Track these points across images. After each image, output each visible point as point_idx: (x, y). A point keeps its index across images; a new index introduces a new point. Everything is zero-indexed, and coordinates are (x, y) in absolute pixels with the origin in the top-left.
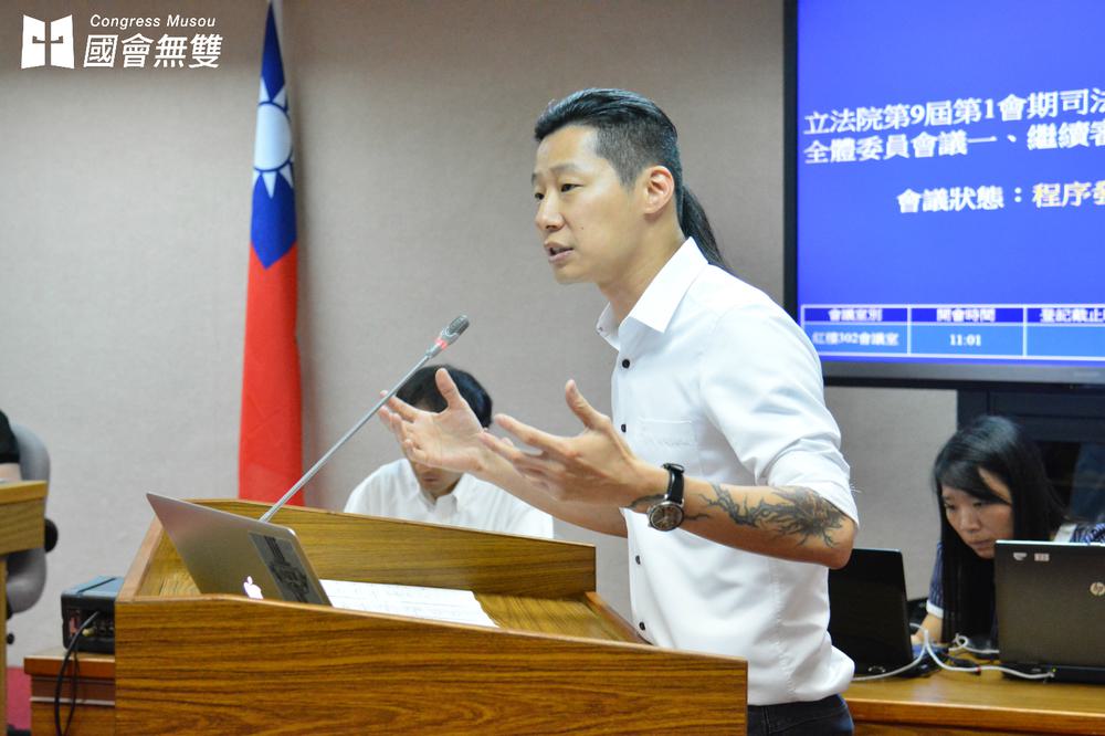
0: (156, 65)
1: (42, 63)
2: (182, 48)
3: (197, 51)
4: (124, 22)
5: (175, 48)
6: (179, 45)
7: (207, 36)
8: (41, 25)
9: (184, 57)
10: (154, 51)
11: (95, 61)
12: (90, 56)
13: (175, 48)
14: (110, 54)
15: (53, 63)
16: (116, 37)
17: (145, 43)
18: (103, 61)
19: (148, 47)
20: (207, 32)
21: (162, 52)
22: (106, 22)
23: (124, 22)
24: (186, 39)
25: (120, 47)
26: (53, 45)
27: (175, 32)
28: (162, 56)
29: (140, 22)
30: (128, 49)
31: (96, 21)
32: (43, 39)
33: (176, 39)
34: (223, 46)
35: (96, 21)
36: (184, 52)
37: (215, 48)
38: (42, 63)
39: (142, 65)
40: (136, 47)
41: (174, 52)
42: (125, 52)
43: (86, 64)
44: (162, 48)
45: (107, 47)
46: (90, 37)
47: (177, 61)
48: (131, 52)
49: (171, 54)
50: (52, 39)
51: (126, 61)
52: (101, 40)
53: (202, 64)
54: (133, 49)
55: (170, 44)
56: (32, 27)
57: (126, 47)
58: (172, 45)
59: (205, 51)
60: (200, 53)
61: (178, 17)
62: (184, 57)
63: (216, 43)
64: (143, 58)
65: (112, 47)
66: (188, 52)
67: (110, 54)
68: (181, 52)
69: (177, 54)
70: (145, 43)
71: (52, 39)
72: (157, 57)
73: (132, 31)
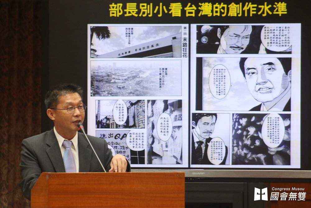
0: (289, 200)
1: (259, 199)
2: (296, 195)
3: (300, 197)
4: (281, 189)
5: (294, 196)
7: (302, 193)
8: (260, 190)
9: (296, 198)
10: (288, 196)
11: (273, 199)
12: (272, 197)
13: (294, 196)
14: (277, 197)
15: (262, 199)
16: (279, 193)
17: (286, 194)
18: (275, 199)
19: (287, 195)
20: (302, 191)
22: (276, 189)
25: (280, 195)
26: (262, 195)
27: (294, 192)
29: (285, 189)
32: (260, 193)
33: (294, 193)
36: (296, 197)
38: (259, 199)
39: (285, 200)
40: (284, 195)
41: (294, 197)
42: (281, 197)
43: (271, 200)
44: (291, 196)
45: (276, 195)
46: (272, 193)
47: (294, 199)
48: (282, 196)
49: (293, 197)
51: (281, 199)
52: (275, 194)
53: (301, 200)
55: (293, 194)
56: (257, 190)
57: (281, 195)
59: (302, 196)
61: (295, 188)
62: (296, 198)
63: (304, 194)
67: (277, 197)
68: (295, 197)
69: (294, 197)
70: (286, 194)
73: (283, 191)
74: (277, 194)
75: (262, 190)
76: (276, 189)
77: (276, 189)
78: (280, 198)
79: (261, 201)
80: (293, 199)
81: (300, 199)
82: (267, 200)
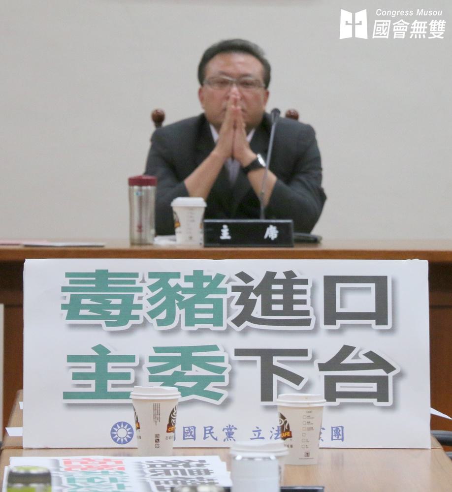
0: (411, 37)
1: (350, 36)
2: (425, 27)
3: (433, 30)
4: (394, 13)
5: (421, 27)
6: (423, 26)
8: (351, 14)
9: (426, 32)
10: (410, 30)
11: (379, 35)
12: (376, 32)
13: (421, 27)
14: (387, 31)
15: (357, 36)
16: (390, 21)
17: (405, 25)
18: (383, 35)
19: (406, 27)
20: (437, 18)
21: (414, 30)
22: (385, 13)
23: (394, 13)
24: (426, 22)
25: (392, 27)
26: (356, 26)
27: (421, 18)
29: (402, 13)
30: (396, 28)
31: (379, 12)
32: (351, 23)
33: (421, 23)
35: (379, 12)
37: (442, 28)
38: (350, 36)
39: (403, 37)
40: (400, 27)
41: (420, 30)
42: (394, 30)
43: (374, 37)
44: (414, 28)
45: (385, 27)
46: (376, 21)
47: (422, 35)
48: (397, 30)
49: (419, 31)
50: (356, 23)
51: (395, 34)
52: (382, 23)
53: (435, 36)
55: (418, 25)
56: (346, 16)
57: (395, 27)
58: (419, 26)
59: (437, 29)
60: (434, 30)
61: (422, 10)
62: (426, 32)
63: (442, 25)
64: (404, 33)
65: (387, 26)
66: (428, 30)
67: (387, 31)
68: (424, 30)
69: (422, 31)
70: (405, 25)
71: (356, 23)
72: (411, 32)
73: (398, 18)
74: (387, 25)
79: (354, 39)
80: (420, 36)
81: (433, 36)
82: (366, 37)
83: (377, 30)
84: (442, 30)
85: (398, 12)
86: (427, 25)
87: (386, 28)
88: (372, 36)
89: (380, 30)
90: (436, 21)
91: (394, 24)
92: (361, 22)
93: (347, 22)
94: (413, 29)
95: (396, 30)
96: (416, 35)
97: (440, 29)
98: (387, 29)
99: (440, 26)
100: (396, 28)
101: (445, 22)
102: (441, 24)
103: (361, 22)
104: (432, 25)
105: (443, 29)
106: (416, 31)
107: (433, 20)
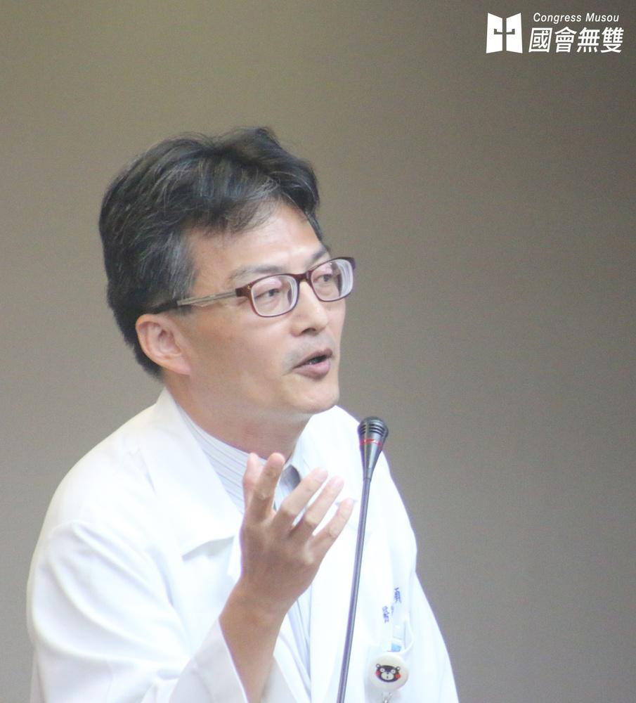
0: (578, 51)
1: (501, 49)
2: (596, 37)
4: (556, 19)
5: (591, 38)
6: (594, 35)
7: (614, 29)
8: (501, 19)
9: (597, 44)
10: (577, 41)
11: (537, 48)
12: (533, 43)
13: (591, 38)
14: (547, 42)
16: (551, 29)
17: (571, 34)
18: (542, 48)
19: (573, 37)
20: (613, 25)
21: (583, 41)
23: (556, 19)
24: (599, 31)
25: (554, 37)
26: (508, 36)
27: (591, 26)
28: (582, 44)
29: (567, 18)
30: (559, 39)
33: (592, 31)
34: (625, 37)
35: (537, 19)
36: (598, 41)
37: (619, 38)
38: (501, 49)
39: (569, 51)
40: (565, 37)
43: (530, 50)
44: (582, 38)
45: (545, 37)
46: (533, 29)
47: (593, 47)
48: (561, 41)
49: (589, 42)
51: (558, 47)
52: (540, 32)
53: (610, 50)
54: (563, 39)
55: (588, 34)
56: (494, 22)
57: (558, 37)
58: (590, 35)
59: (612, 40)
60: (608, 41)
61: (593, 14)
62: (597, 44)
63: (619, 34)
64: (570, 45)
65: (548, 36)
66: (600, 41)
67: (547, 42)
69: (593, 42)
70: (571, 34)
72: (579, 44)
75: (507, 19)
76: (544, 18)
77: (544, 18)
78: (554, 45)
79: (504, 54)
81: (606, 48)
82: (520, 51)
83: (535, 41)
84: (618, 41)
85: (562, 17)
86: (599, 34)
87: (546, 38)
88: (528, 50)
89: (539, 41)
90: (611, 28)
91: (556, 33)
92: (513, 30)
93: (495, 30)
94: (581, 40)
95: (559, 41)
96: (585, 48)
97: (616, 40)
98: (548, 39)
99: (617, 36)
100: (559, 39)
101: (623, 31)
102: (617, 32)
103: (513, 30)
104: (606, 35)
105: (620, 40)
106: (585, 42)
107: (607, 28)
